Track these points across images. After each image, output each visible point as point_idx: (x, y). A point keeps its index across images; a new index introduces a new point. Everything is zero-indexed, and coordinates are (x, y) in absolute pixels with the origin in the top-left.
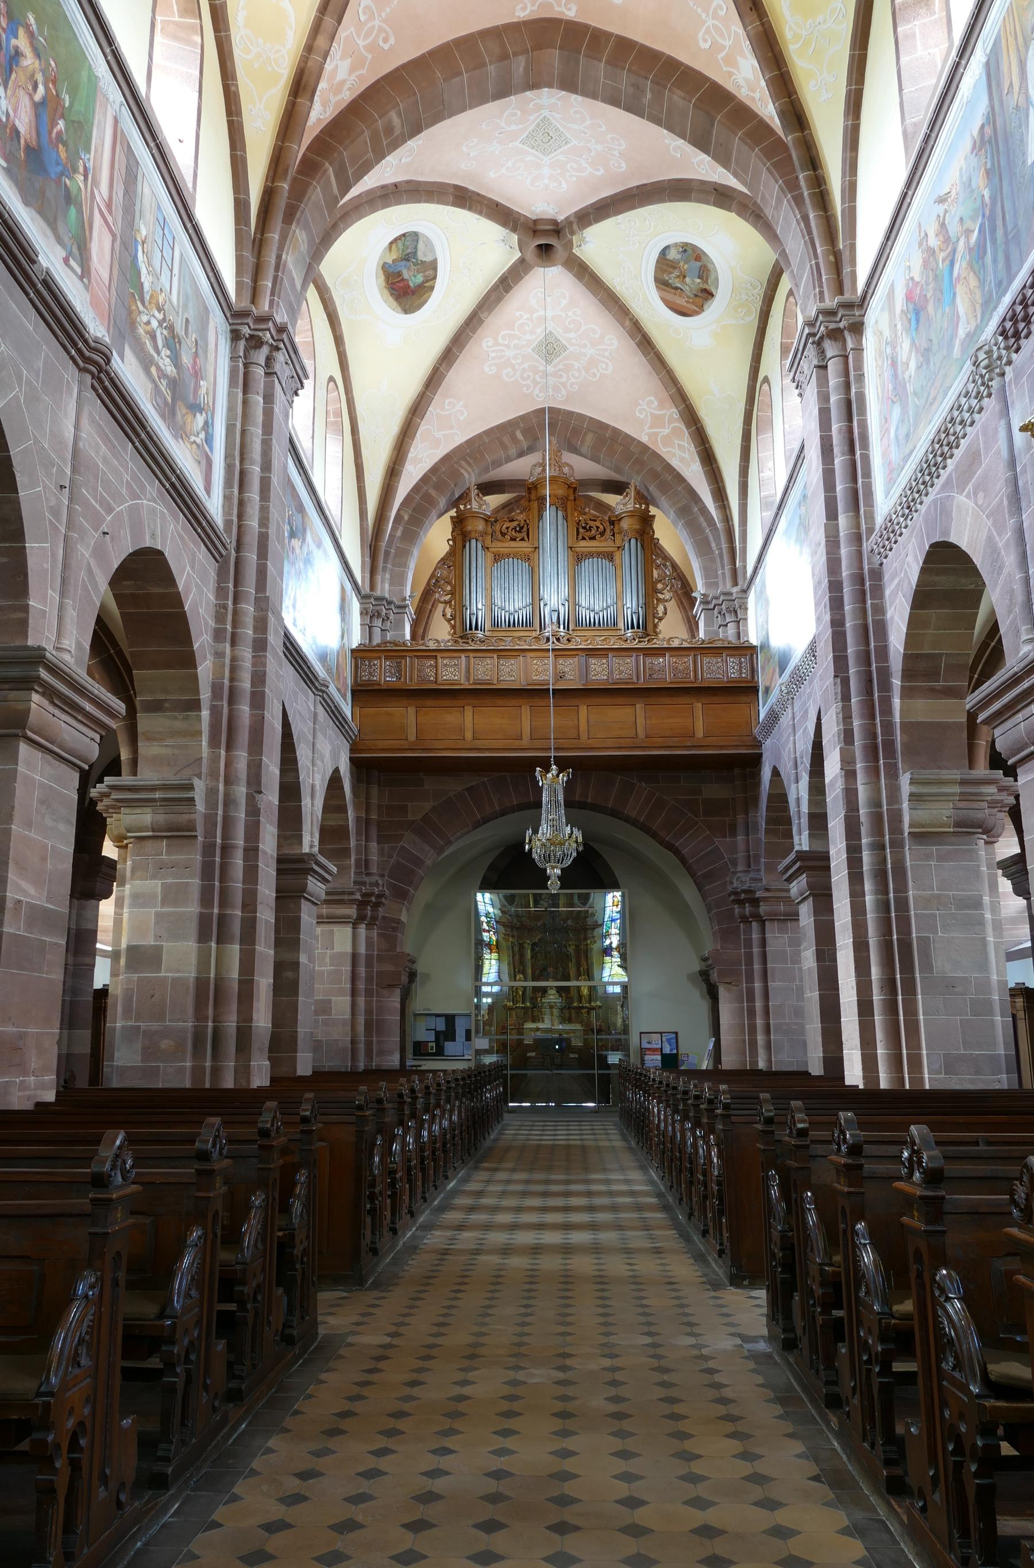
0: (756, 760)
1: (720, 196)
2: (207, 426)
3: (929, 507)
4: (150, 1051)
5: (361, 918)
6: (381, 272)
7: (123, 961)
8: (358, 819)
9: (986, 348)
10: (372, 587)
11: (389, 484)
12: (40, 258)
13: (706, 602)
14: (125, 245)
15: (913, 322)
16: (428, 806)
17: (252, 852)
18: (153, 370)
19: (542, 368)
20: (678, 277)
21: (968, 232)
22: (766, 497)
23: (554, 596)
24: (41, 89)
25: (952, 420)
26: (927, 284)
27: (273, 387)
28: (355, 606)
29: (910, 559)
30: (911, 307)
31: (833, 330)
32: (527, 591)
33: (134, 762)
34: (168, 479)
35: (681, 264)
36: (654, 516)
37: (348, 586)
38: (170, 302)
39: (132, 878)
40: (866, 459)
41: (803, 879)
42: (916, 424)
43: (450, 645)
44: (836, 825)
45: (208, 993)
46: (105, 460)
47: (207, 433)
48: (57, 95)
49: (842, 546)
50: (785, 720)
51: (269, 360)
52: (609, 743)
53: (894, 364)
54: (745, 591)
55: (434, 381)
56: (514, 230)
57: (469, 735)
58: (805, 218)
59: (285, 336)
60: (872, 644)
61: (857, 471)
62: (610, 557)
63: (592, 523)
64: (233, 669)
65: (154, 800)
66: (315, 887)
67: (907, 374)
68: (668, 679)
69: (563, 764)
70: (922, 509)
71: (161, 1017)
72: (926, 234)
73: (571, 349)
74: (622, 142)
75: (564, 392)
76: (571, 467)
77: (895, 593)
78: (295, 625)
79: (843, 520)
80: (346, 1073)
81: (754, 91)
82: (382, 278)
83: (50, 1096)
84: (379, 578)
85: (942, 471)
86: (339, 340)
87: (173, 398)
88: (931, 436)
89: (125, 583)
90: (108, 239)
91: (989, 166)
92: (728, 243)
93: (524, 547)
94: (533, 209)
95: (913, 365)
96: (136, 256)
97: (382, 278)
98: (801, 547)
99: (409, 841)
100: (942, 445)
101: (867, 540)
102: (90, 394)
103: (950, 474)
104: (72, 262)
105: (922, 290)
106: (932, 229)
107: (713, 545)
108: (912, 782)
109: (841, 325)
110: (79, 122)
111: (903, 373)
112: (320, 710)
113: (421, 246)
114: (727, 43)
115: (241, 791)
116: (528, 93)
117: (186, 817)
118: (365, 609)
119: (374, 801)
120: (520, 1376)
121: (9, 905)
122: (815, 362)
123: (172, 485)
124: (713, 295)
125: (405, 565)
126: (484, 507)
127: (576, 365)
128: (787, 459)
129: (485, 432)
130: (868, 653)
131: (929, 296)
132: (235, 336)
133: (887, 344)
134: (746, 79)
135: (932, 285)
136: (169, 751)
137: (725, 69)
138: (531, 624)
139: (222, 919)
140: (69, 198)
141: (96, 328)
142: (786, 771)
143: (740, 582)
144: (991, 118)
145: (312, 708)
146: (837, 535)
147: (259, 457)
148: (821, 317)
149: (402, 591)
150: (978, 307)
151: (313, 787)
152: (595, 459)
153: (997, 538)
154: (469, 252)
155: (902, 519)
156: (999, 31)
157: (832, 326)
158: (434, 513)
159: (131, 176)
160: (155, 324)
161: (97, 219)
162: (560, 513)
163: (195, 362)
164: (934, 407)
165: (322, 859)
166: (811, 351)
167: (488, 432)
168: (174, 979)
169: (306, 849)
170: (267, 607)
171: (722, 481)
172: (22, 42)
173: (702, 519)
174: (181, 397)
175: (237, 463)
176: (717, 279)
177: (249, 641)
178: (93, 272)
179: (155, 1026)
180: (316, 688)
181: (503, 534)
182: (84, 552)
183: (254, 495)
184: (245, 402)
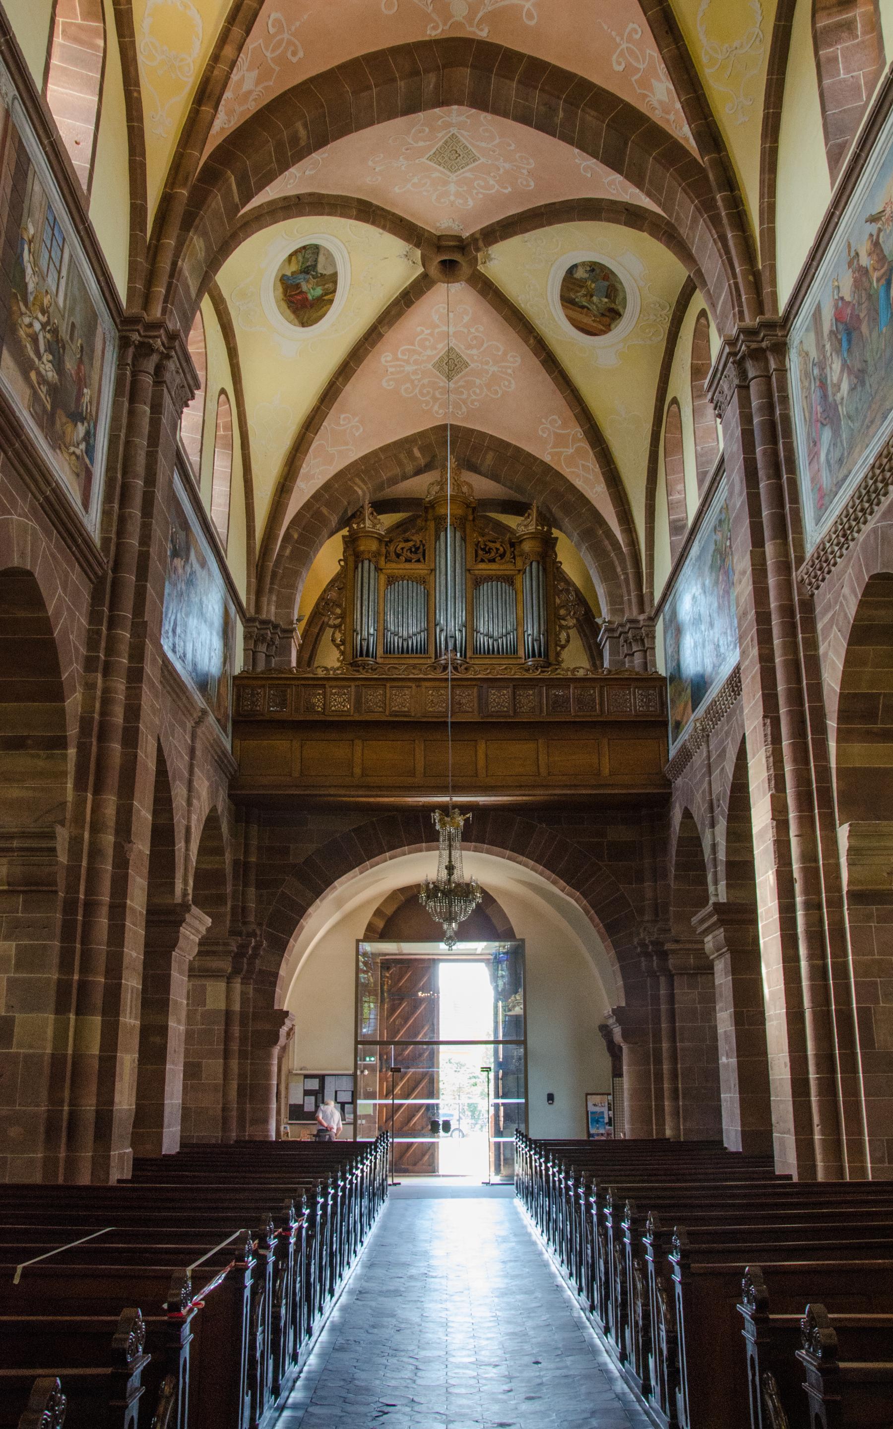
1: (632, 216)
2: (89, 437)
3: (868, 536)
6: (279, 284)
11: (278, 502)
15: (845, 344)
18: (33, 375)
19: (442, 384)
20: (585, 295)
22: (675, 521)
26: (860, 304)
27: (161, 396)
29: (846, 590)
30: (841, 327)
31: (756, 350)
34: (42, 493)
35: (589, 283)
36: (556, 539)
37: (233, 609)
42: (851, 448)
47: (88, 444)
49: (770, 575)
50: (698, 759)
53: (823, 385)
54: (653, 619)
55: (330, 395)
56: (418, 245)
58: (723, 238)
60: (805, 682)
61: (785, 497)
62: (510, 580)
63: (491, 545)
67: (839, 396)
68: (573, 712)
70: (861, 537)
72: (857, 254)
73: (472, 365)
74: (531, 161)
75: (464, 409)
77: (828, 628)
81: (668, 113)
82: (280, 290)
84: (265, 600)
92: (639, 263)
93: (420, 569)
94: (438, 225)
95: (845, 386)
100: (883, 471)
101: (797, 570)
105: (853, 309)
106: (864, 249)
107: (619, 569)
109: (764, 344)
111: (834, 395)
113: (321, 259)
114: (642, 67)
118: (250, 633)
123: (47, 499)
125: (293, 587)
126: (378, 526)
127: (478, 381)
128: (700, 482)
129: (381, 449)
131: (862, 315)
132: (124, 343)
133: (814, 365)
137: (639, 91)
138: (426, 651)
142: (699, 811)
143: (647, 609)
146: (764, 564)
147: (146, 470)
148: (742, 337)
149: (290, 615)
152: (495, 477)
154: (369, 266)
155: (836, 548)
157: (754, 345)
158: (325, 532)
160: (37, 326)
162: (458, 535)
164: (871, 431)
167: (384, 449)
170: (144, 630)
173: (606, 542)
175: (119, 476)
176: (625, 299)
181: (398, 556)
183: (136, 511)
184: (132, 412)
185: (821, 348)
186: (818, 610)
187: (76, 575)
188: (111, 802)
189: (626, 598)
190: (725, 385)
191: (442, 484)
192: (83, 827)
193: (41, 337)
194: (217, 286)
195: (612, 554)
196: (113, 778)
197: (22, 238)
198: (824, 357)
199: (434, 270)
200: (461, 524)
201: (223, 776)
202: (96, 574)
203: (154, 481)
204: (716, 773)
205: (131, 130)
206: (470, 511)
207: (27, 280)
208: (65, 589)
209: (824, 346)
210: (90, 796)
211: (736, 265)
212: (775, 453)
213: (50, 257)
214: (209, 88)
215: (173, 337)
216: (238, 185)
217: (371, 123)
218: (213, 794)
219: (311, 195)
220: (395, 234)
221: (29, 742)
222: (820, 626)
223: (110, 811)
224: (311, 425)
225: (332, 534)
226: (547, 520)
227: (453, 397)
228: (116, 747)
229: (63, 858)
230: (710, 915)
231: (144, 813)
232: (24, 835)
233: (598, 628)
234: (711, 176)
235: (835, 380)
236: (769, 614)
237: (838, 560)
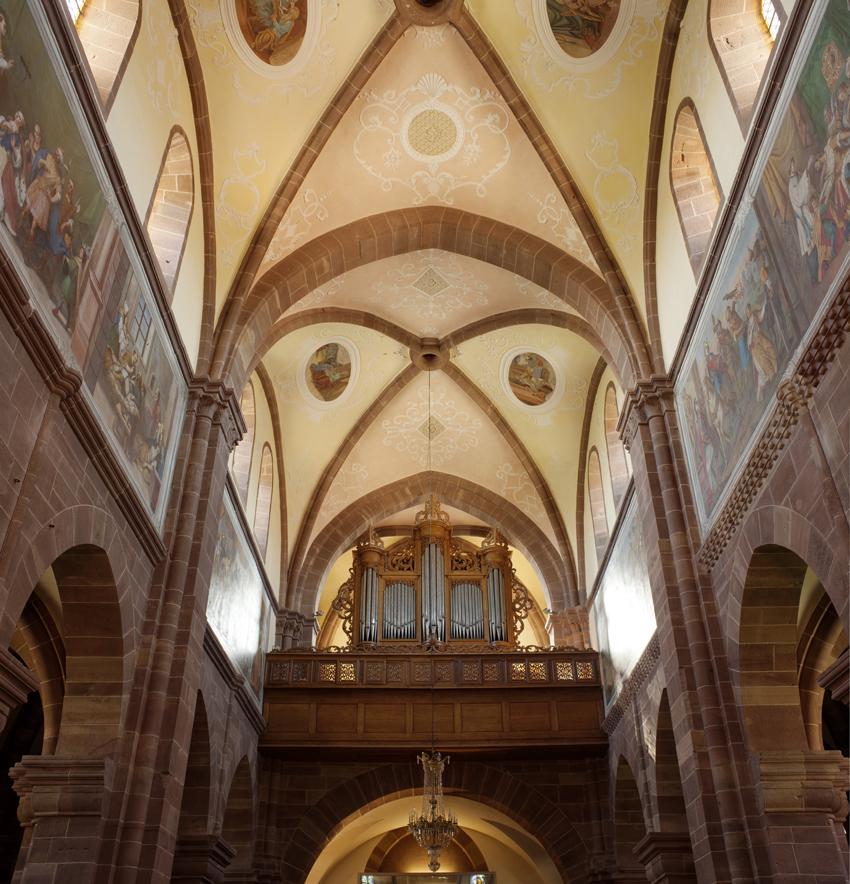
0: (602, 751)
1: (556, 318)
2: (159, 458)
6: (309, 371)
9: (789, 385)
10: (288, 604)
11: (306, 525)
12: (30, 301)
14: (109, 313)
18: (119, 406)
21: (756, 313)
24: (58, 196)
25: (765, 446)
27: (217, 434)
28: (273, 619)
29: (736, 564)
30: (712, 374)
31: (651, 398)
33: (55, 741)
34: (118, 491)
35: (528, 368)
36: (511, 552)
37: (268, 602)
38: (141, 361)
40: (687, 490)
41: (658, 860)
44: (694, 805)
47: (159, 463)
48: (71, 203)
49: (675, 558)
50: (629, 715)
51: (217, 415)
53: (704, 416)
54: (586, 611)
55: (345, 449)
56: (407, 344)
57: (361, 728)
58: (622, 326)
59: (230, 398)
62: (478, 583)
67: (717, 421)
75: (442, 461)
76: (446, 514)
77: (725, 595)
78: (219, 628)
79: (674, 538)
82: (310, 375)
84: (293, 597)
85: (758, 489)
86: (275, 418)
87: (133, 429)
88: (746, 462)
89: (71, 578)
91: (767, 265)
92: (559, 350)
93: (410, 575)
95: (720, 414)
96: (118, 323)
98: (634, 570)
102: (57, 411)
103: (767, 489)
104: (60, 314)
107: (559, 573)
109: (657, 394)
110: (86, 225)
112: (235, 703)
113: (340, 353)
114: (558, 220)
116: (419, 251)
122: (639, 421)
123: (121, 496)
124: (551, 390)
126: (379, 544)
127: (452, 440)
129: (382, 488)
132: (192, 396)
134: (572, 240)
135: (729, 355)
137: (557, 235)
138: (415, 637)
141: (71, 361)
143: (581, 601)
144: (764, 233)
145: (228, 700)
146: (670, 550)
147: (200, 489)
148: (640, 389)
150: (774, 362)
153: (822, 535)
154: (374, 360)
155: (725, 532)
156: (762, 180)
157: (650, 395)
158: (340, 549)
159: (123, 269)
161: (88, 291)
163: (156, 409)
166: (634, 414)
167: (384, 489)
170: (194, 605)
171: (563, 524)
172: (49, 163)
173: (549, 554)
174: (140, 430)
175: (182, 488)
176: (554, 379)
178: (77, 325)
180: (233, 683)
181: (394, 566)
183: (193, 515)
184: (194, 444)
185: (699, 390)
187: (141, 558)
188: (154, 739)
189: (565, 594)
190: (630, 425)
192: (129, 760)
193: (127, 382)
195: (554, 563)
196: (158, 720)
197: (119, 313)
198: (703, 397)
199: (419, 360)
201: (255, 733)
202: (157, 558)
203: (208, 494)
205: (207, 259)
206: (447, 533)
207: (120, 341)
208: (131, 568)
209: (702, 389)
210: (137, 734)
211: (632, 341)
212: (672, 469)
213: (139, 329)
214: (263, 233)
216: (280, 298)
217: (374, 260)
219: (332, 308)
220: (391, 336)
221: (92, 688)
222: (718, 595)
223: (153, 746)
224: (330, 471)
225: (346, 550)
228: (162, 694)
229: (108, 786)
231: (182, 751)
232: (79, 766)
234: (610, 285)
235: (712, 411)
237: (728, 541)
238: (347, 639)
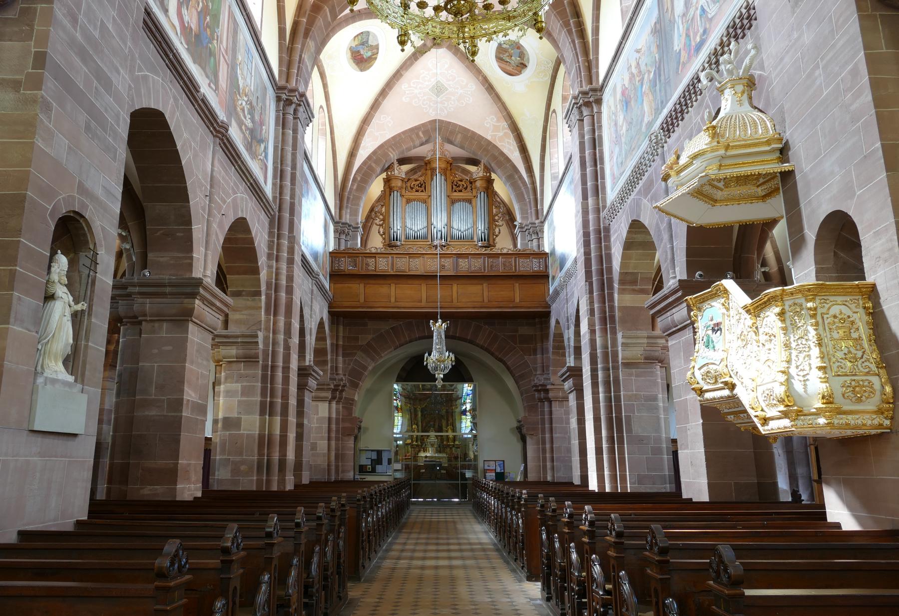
0: (547, 315)
2: (266, 148)
4: (235, 471)
5: (333, 398)
7: (220, 425)
8: (332, 344)
10: (340, 217)
13: (521, 227)
16: (370, 337)
17: (286, 369)
21: (649, 72)
23: (440, 221)
28: (331, 228)
29: (622, 225)
32: (425, 219)
34: (249, 181)
37: (328, 218)
39: (225, 382)
40: (602, 169)
41: (571, 381)
42: (626, 157)
43: (383, 251)
45: (264, 442)
46: (223, 178)
50: (562, 295)
51: (295, 111)
52: (469, 305)
53: (616, 124)
54: (543, 222)
55: (375, 105)
57: (393, 300)
58: (573, 41)
61: (598, 176)
62: (469, 201)
64: (277, 274)
65: (237, 343)
66: (312, 383)
68: (501, 270)
69: (445, 317)
71: (241, 454)
79: (591, 201)
80: (325, 482)
83: (199, 494)
84: (344, 212)
86: (325, 86)
90: (225, 67)
93: (423, 195)
95: (624, 128)
97: (349, 54)
99: (360, 356)
102: (218, 148)
106: (634, 64)
108: (623, 337)
109: (591, 100)
112: (315, 288)
113: (371, 38)
115: (281, 337)
117: (254, 351)
119: (341, 334)
120: (437, 611)
121: (185, 402)
122: (578, 117)
123: (251, 184)
125: (358, 205)
130: (602, 270)
132: (278, 99)
136: (245, 317)
138: (427, 238)
139: (271, 403)
140: (211, 54)
141: (222, 116)
142: (563, 322)
146: (588, 208)
149: (356, 219)
151: (311, 329)
152: (462, 147)
157: (586, 100)
158: (374, 176)
160: (244, 103)
165: (316, 368)
167: (404, 133)
168: (248, 435)
169: (307, 364)
170: (293, 240)
174: (254, 138)
177: (285, 260)
179: (238, 458)
181: (412, 188)
182: (215, 226)
183: (288, 183)
184: (283, 134)
186: (612, 232)
191: (434, 151)
194: (320, 61)
200: (444, 172)
204: (570, 303)
215: (303, 95)
218: (321, 312)
222: (612, 239)
224: (366, 121)
226: (488, 169)
227: (439, 105)
228: (283, 295)
230: (566, 372)
231: (296, 325)
233: (515, 226)
236: (589, 233)
238: (381, 239)
